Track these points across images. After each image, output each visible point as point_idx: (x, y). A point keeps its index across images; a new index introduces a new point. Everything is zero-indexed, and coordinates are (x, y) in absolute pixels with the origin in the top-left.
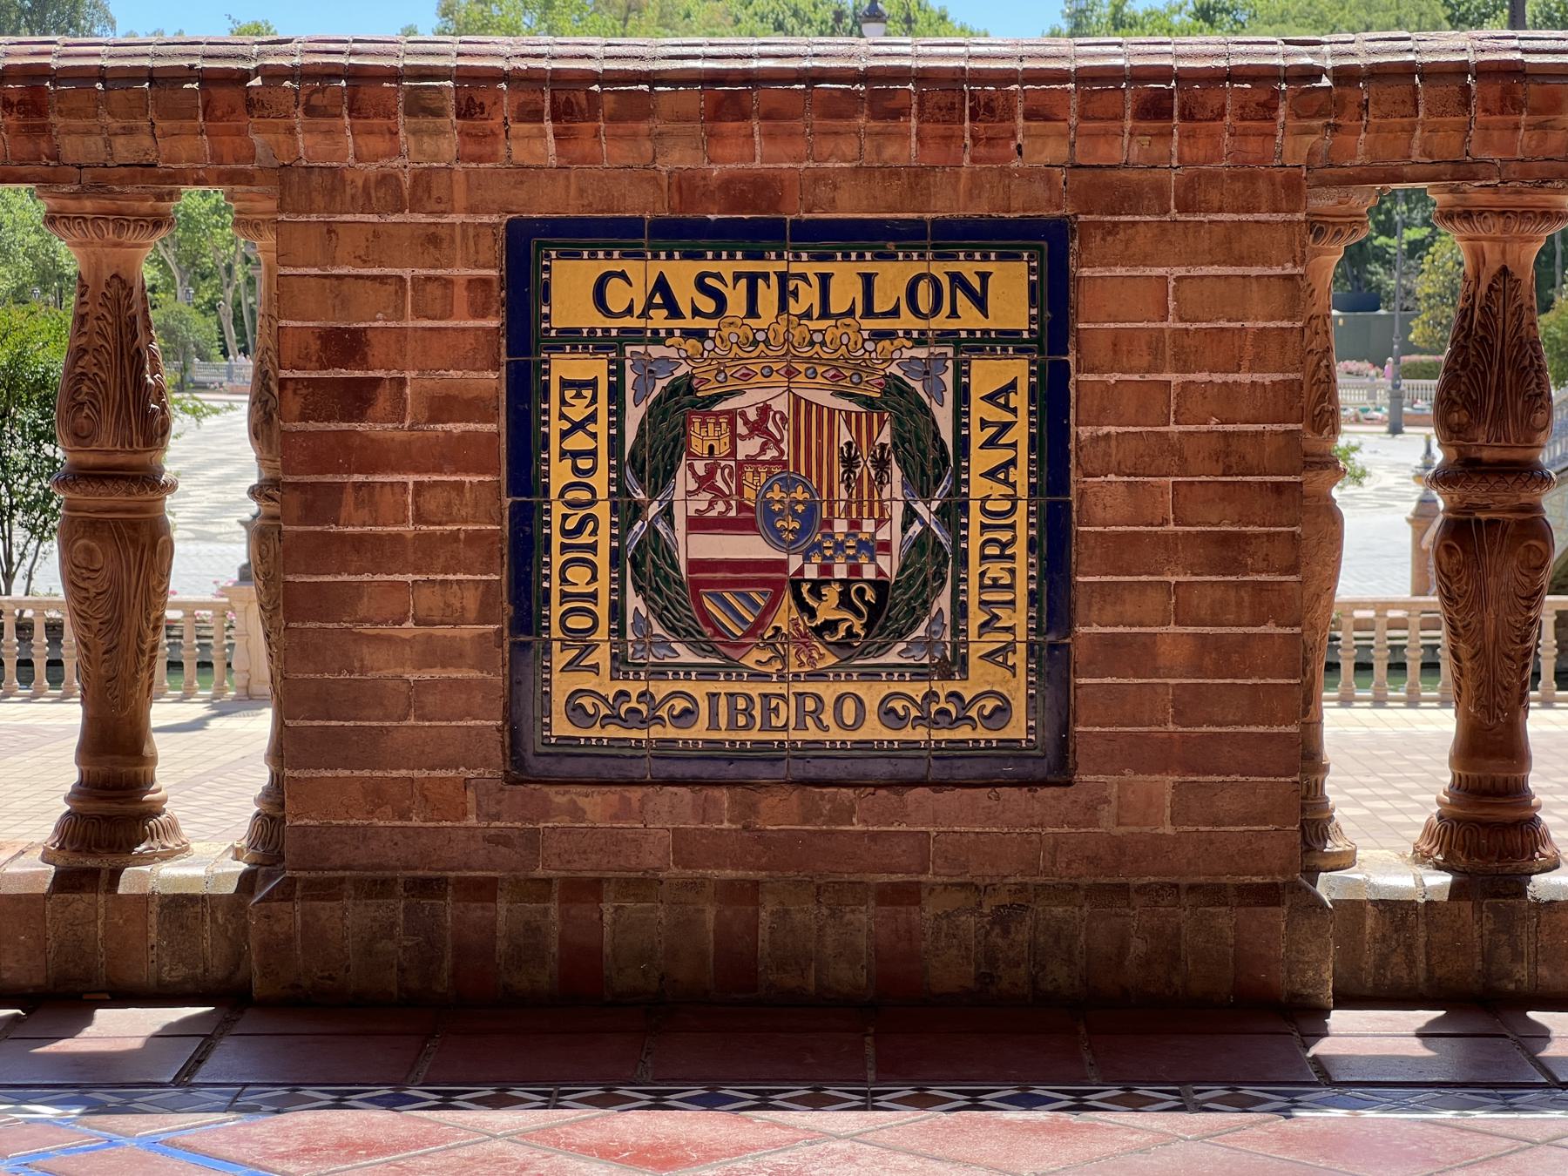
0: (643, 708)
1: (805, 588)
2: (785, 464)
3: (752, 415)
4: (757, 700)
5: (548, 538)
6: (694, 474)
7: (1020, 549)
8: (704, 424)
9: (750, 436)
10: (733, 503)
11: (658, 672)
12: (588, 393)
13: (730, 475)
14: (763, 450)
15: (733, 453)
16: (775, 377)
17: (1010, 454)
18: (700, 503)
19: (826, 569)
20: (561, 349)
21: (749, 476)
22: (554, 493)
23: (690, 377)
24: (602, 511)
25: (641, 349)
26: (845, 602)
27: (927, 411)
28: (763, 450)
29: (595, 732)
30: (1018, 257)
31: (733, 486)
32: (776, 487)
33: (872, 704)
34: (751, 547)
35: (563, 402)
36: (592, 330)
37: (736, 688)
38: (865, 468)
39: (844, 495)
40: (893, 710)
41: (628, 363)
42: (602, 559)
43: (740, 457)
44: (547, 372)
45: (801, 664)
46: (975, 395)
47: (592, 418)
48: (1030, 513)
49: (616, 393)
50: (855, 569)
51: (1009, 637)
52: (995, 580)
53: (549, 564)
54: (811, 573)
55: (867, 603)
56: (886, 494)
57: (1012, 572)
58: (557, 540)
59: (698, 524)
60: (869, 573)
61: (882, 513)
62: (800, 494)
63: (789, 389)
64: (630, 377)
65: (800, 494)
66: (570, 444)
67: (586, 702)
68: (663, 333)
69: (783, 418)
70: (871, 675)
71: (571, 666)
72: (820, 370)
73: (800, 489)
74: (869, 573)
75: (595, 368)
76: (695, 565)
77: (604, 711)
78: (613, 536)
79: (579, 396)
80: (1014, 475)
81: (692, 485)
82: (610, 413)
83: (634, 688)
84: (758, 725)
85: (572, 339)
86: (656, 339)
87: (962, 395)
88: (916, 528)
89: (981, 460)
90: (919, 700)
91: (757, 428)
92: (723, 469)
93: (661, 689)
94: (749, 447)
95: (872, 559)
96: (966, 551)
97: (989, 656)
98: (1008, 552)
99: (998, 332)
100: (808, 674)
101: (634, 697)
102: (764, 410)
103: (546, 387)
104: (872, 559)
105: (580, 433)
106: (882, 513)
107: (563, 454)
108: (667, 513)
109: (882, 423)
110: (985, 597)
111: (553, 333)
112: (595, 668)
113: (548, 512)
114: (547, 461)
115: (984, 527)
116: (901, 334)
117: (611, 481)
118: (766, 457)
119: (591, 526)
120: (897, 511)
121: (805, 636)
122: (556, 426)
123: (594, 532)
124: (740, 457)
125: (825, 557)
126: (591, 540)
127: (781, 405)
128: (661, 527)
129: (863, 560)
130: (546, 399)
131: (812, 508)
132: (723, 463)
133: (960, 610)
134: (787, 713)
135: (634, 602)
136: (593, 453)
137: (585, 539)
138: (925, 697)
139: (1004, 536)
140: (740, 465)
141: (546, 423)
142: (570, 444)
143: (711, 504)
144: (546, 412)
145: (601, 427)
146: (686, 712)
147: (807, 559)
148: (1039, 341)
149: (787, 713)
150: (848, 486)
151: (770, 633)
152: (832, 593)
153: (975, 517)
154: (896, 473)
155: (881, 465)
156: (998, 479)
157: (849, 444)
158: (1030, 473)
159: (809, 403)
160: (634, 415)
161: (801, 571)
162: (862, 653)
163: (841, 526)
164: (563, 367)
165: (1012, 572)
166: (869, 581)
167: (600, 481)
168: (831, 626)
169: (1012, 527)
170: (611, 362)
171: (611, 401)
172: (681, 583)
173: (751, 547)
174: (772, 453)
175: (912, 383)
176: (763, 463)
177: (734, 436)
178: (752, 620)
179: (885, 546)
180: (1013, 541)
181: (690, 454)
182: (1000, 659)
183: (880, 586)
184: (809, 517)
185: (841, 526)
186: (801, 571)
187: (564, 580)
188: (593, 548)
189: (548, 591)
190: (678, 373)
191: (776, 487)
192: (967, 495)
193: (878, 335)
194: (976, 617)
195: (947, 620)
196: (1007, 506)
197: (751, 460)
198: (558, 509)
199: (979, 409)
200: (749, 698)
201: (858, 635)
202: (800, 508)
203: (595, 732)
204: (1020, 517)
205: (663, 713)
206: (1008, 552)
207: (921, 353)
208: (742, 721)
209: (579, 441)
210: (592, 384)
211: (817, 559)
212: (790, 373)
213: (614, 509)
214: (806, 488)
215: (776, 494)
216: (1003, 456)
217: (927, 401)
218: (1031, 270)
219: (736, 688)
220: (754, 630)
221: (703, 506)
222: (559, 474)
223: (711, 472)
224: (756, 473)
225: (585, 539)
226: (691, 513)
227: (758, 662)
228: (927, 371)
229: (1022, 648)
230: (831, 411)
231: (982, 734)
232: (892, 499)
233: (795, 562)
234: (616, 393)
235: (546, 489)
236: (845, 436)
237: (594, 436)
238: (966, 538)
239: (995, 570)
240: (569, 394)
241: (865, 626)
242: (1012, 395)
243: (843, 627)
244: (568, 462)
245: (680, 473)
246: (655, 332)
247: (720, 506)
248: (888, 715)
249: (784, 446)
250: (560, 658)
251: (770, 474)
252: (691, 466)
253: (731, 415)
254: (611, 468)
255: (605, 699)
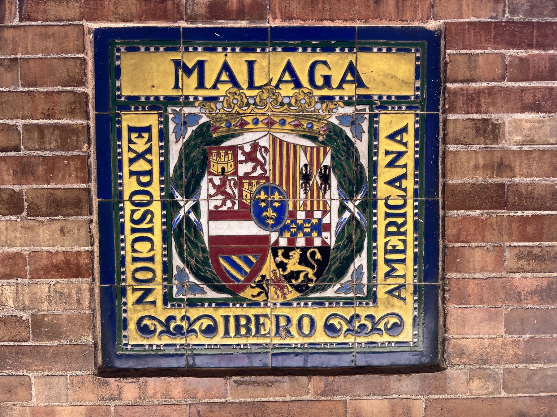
0: (185, 324)
1: (280, 252)
2: (268, 179)
3: (247, 149)
4: (253, 319)
5: (123, 225)
6: (214, 185)
7: (409, 227)
8: (218, 154)
9: (246, 161)
10: (237, 202)
11: (192, 303)
12: (146, 135)
13: (234, 184)
14: (254, 169)
15: (235, 173)
16: (260, 125)
17: (401, 171)
18: (216, 202)
19: (292, 241)
20: (128, 109)
21: (246, 186)
22: (126, 196)
23: (207, 125)
24: (156, 207)
25: (178, 109)
26: (303, 260)
27: (353, 144)
28: (254, 169)
29: (155, 341)
30: (409, 51)
31: (236, 191)
32: (262, 193)
33: (320, 324)
34: (248, 228)
35: (130, 141)
36: (147, 98)
37: (239, 311)
38: (316, 180)
39: (303, 196)
40: (332, 325)
41: (171, 116)
42: (157, 237)
43: (241, 173)
44: (120, 122)
45: (278, 297)
46: (383, 134)
47: (149, 151)
48: (415, 207)
49: (163, 135)
50: (309, 241)
51: (401, 281)
52: (394, 246)
53: (123, 241)
54: (283, 242)
55: (317, 261)
56: (327, 196)
57: (404, 242)
58: (128, 225)
59: (215, 215)
60: (317, 242)
61: (325, 206)
62: (277, 196)
63: (269, 133)
64: (172, 126)
65: (277, 196)
66: (136, 167)
67: (146, 322)
68: (191, 99)
69: (267, 151)
70: (319, 303)
71: (140, 301)
72: (288, 120)
73: (277, 193)
74: (317, 242)
75: (151, 120)
76: (212, 239)
77: (160, 328)
78: (163, 224)
79: (140, 136)
80: (405, 183)
81: (212, 191)
82: (161, 148)
83: (178, 313)
84: (253, 334)
85: (133, 102)
86: (187, 102)
87: (374, 134)
88: (347, 215)
89: (386, 173)
90: (348, 318)
91: (250, 157)
92: (230, 181)
93: (194, 313)
94: (245, 168)
95: (320, 235)
96: (376, 230)
97: (390, 292)
98: (402, 230)
99: (398, 97)
100: (282, 304)
101: (178, 318)
102: (255, 146)
103: (119, 131)
104: (320, 235)
105: (141, 161)
106: (325, 206)
107: (132, 173)
108: (196, 209)
109: (325, 154)
110: (389, 257)
111: (123, 99)
112: (154, 303)
113: (122, 209)
114: (121, 177)
115: (387, 215)
116: (337, 99)
117: (162, 190)
118: (255, 174)
119: (149, 217)
120: (335, 206)
121: (279, 281)
122: (126, 156)
123: (151, 221)
124: (241, 173)
125: (292, 235)
126: (149, 226)
127: (264, 142)
128: (192, 216)
129: (315, 234)
130: (120, 138)
131: (283, 203)
132: (229, 178)
133: (373, 266)
134: (269, 325)
135: (177, 261)
136: (149, 173)
137: (143, 226)
138: (352, 317)
139: (400, 220)
140: (241, 178)
141: (120, 154)
142: (136, 167)
143: (224, 203)
144: (120, 147)
145: (155, 158)
146: (209, 326)
147: (281, 235)
148: (421, 103)
149: (269, 325)
150: (305, 189)
151: (258, 279)
152: (296, 255)
153: (381, 208)
154: (334, 181)
155: (325, 179)
156: (395, 185)
157: (306, 166)
158: (416, 183)
159: (281, 142)
160: (175, 150)
161: (277, 242)
162: (315, 289)
163: (301, 216)
164: (129, 119)
165: (404, 242)
166: (317, 248)
167: (155, 189)
168: (295, 275)
169: (404, 215)
170: (160, 115)
171: (161, 139)
172: (204, 250)
173: (248, 228)
174: (259, 171)
175: (344, 128)
176: (254, 178)
177: (236, 162)
178: (248, 270)
179: (328, 227)
180: (404, 224)
181: (210, 173)
182: (397, 294)
183: (325, 249)
184: (280, 211)
185: (301, 216)
186: (277, 242)
187: (134, 251)
188: (151, 230)
189: (123, 257)
190: (201, 121)
191: (262, 193)
192: (375, 196)
193: (323, 99)
194: (383, 269)
195: (365, 270)
196: (401, 202)
197: (247, 175)
198: (128, 207)
199: (385, 144)
200: (248, 319)
201: (311, 281)
202: (277, 205)
203: (155, 341)
204: (409, 210)
205: (196, 327)
206: (402, 230)
207: (349, 110)
208: (243, 331)
209: (141, 166)
210: (148, 129)
211: (288, 235)
212: (270, 123)
213: (164, 207)
214: (280, 193)
215: (263, 196)
216: (396, 172)
217: (353, 140)
218: (417, 59)
219: (239, 311)
220: (250, 277)
221: (219, 203)
222: (130, 185)
223: (224, 183)
224: (250, 184)
225: (143, 226)
226: (211, 208)
227: (253, 296)
228: (354, 121)
229: (411, 289)
230: (295, 146)
231: (386, 338)
232: (331, 200)
233: (274, 236)
234: (163, 135)
235: (121, 194)
236: (303, 160)
237: (150, 162)
238: (375, 222)
239: (394, 240)
240: (134, 136)
241: (315, 274)
242: (404, 134)
243: (302, 275)
244: (134, 178)
245: (204, 183)
246: (187, 97)
247: (229, 204)
248: (330, 328)
249: (267, 167)
250: (131, 298)
251: (258, 183)
252: (211, 181)
253: (234, 148)
254: (161, 182)
255: (160, 321)
